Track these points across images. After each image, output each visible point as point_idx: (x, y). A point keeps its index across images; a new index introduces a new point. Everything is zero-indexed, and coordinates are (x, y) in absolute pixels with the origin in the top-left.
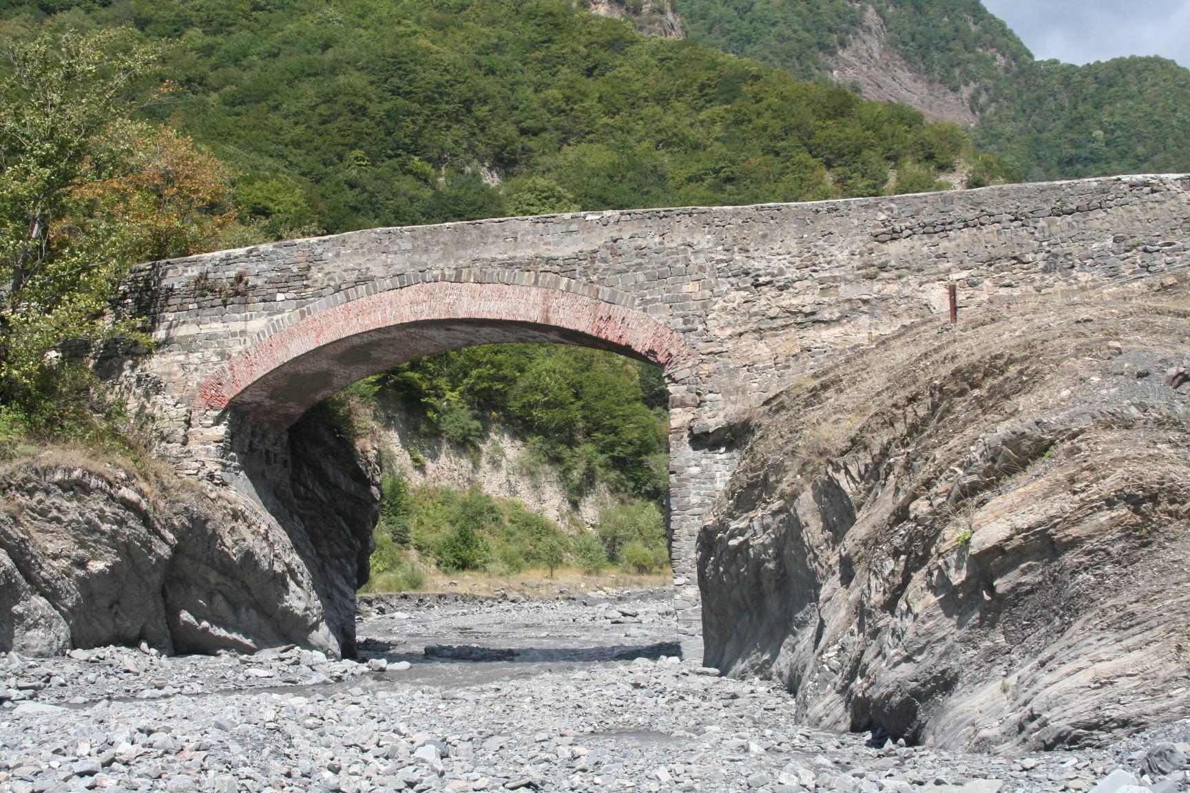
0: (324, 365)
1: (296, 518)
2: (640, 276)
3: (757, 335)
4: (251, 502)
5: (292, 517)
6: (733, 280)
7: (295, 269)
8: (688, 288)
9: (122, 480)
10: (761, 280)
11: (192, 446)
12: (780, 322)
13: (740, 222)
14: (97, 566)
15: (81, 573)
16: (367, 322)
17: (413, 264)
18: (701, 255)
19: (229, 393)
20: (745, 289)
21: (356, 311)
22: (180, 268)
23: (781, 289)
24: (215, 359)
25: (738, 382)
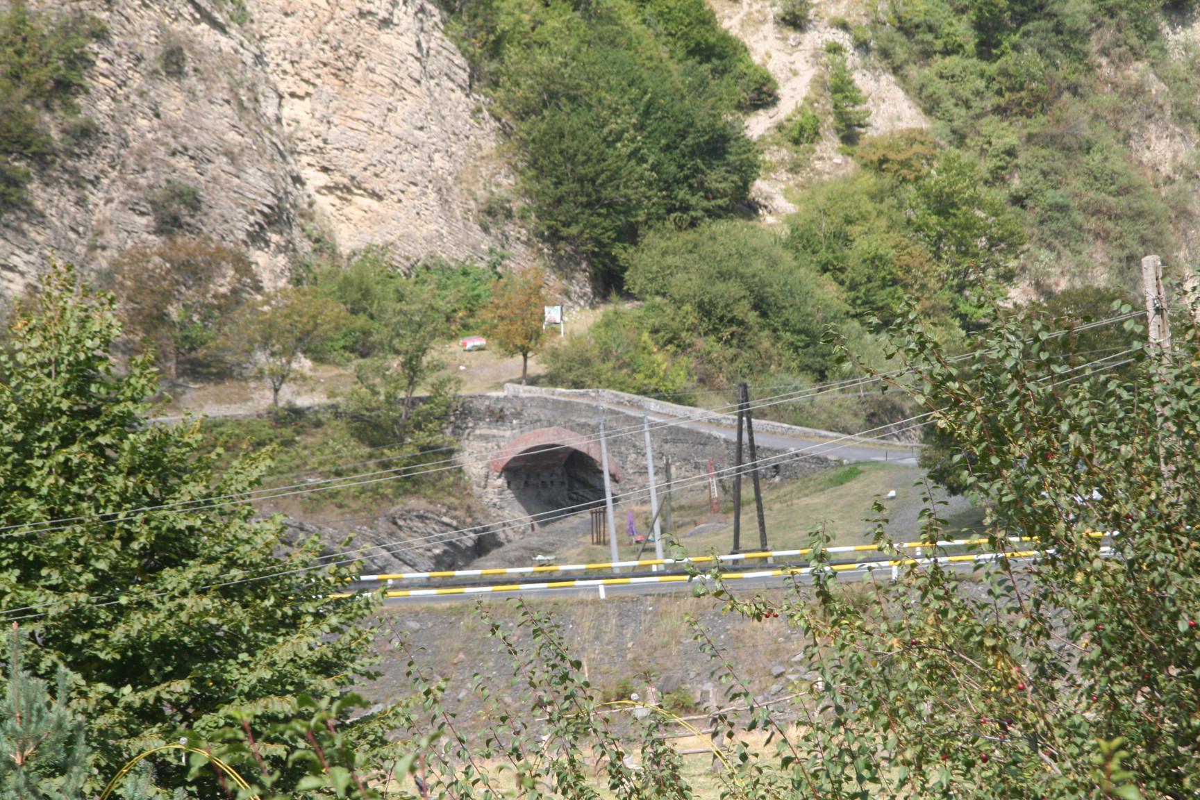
8: (623, 449)
11: (489, 489)
14: (437, 551)
15: (429, 554)
19: (502, 465)
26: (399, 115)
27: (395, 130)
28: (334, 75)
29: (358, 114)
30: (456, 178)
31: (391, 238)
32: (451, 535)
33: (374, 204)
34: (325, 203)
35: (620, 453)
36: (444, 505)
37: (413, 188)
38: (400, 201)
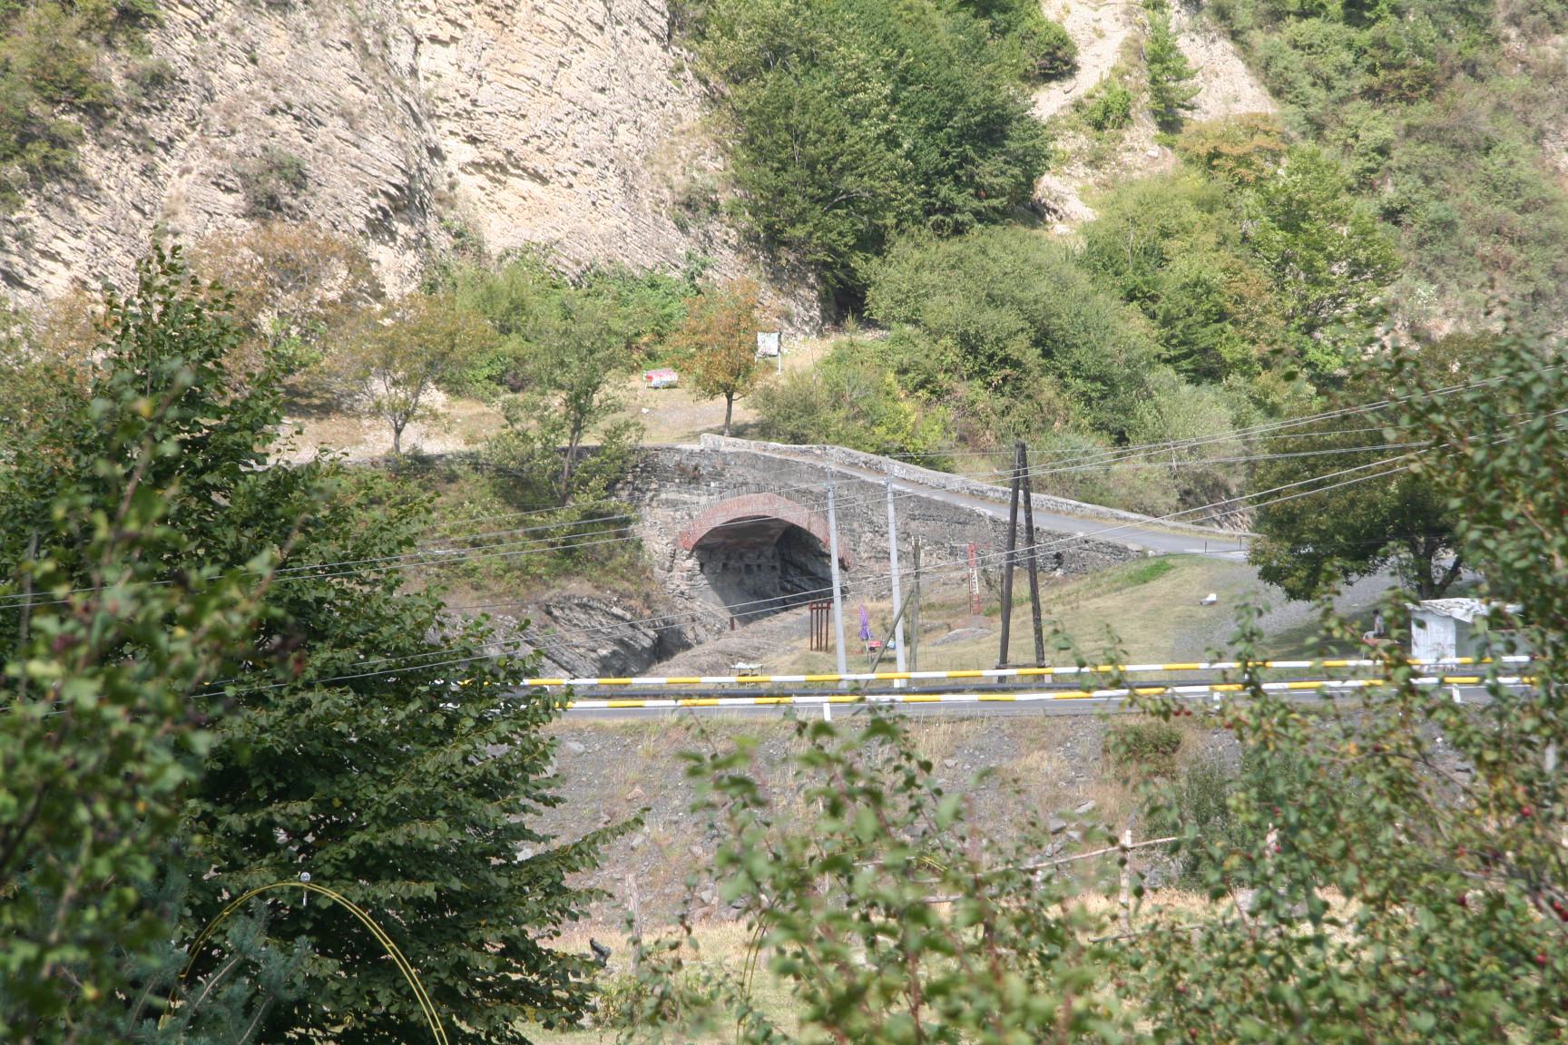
4: (711, 607)
8: (855, 525)
11: (676, 573)
14: (603, 652)
15: (593, 655)
26: (574, 71)
27: (568, 91)
28: (489, 14)
29: (519, 68)
30: (646, 158)
31: (556, 235)
32: (624, 631)
33: (536, 188)
34: (470, 185)
36: (615, 591)
37: (588, 169)
38: (571, 186)
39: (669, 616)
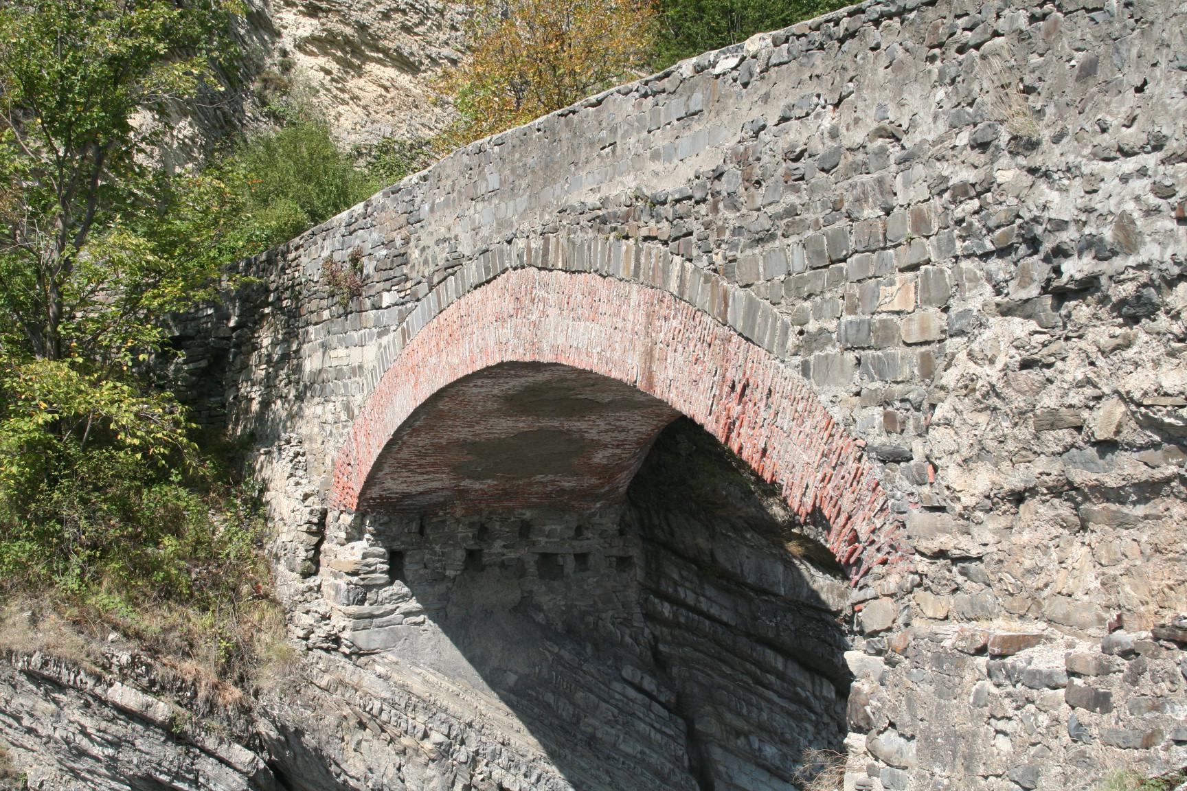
0: (504, 426)
1: (627, 672)
2: (799, 260)
3: (1065, 509)
5: (619, 670)
6: (994, 264)
7: (399, 242)
9: (121, 668)
10: (1073, 269)
11: (324, 577)
12: (1128, 467)
13: (1023, 22)
16: (456, 361)
17: (502, 224)
18: (919, 170)
20: (1021, 309)
21: (445, 335)
22: (320, 242)
23: (1134, 311)
24: (344, 417)
25: (959, 715)
31: (427, 134)
33: (405, 79)
34: (310, 66)
35: (868, 341)
39: (290, 714)
